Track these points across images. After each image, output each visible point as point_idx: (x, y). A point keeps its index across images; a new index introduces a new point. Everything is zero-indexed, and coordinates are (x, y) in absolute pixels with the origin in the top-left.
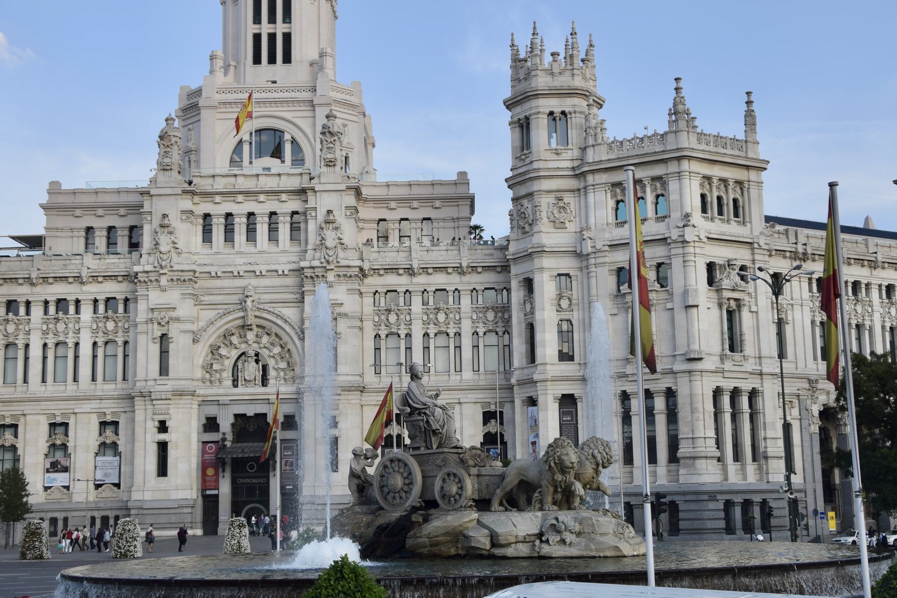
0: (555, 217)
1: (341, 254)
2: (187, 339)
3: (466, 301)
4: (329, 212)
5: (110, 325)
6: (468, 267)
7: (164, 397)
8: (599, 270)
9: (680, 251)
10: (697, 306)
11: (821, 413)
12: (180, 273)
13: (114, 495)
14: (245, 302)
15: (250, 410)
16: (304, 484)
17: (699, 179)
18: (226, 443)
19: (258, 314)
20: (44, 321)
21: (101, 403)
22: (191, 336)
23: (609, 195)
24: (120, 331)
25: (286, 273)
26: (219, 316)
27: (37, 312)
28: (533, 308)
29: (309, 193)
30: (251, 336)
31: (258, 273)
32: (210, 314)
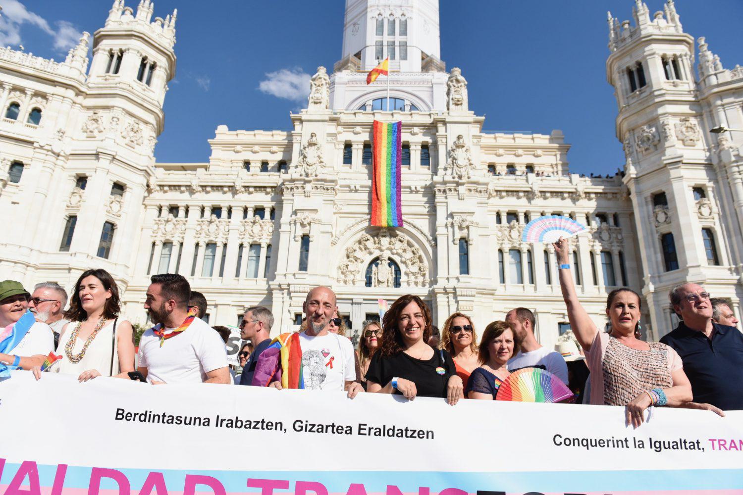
1: (471, 173)
2: (328, 239)
4: (459, 137)
5: (256, 228)
12: (323, 183)
20: (199, 223)
21: (241, 297)
26: (357, 221)
29: (440, 125)
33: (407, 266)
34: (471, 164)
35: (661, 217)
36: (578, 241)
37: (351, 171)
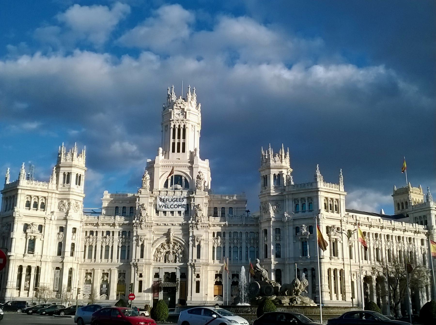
1: (202, 219)
3: (244, 236)
4: (199, 205)
6: (245, 225)
7: (142, 265)
8: (290, 227)
11: (364, 278)
13: (123, 298)
14: (170, 234)
15: (170, 271)
16: (188, 297)
18: (162, 282)
19: (174, 238)
23: (293, 202)
24: (127, 243)
25: (184, 224)
27: (100, 235)
28: (267, 239)
30: (171, 246)
33: (179, 255)
34: (203, 216)
35: (265, 238)
36: (242, 243)
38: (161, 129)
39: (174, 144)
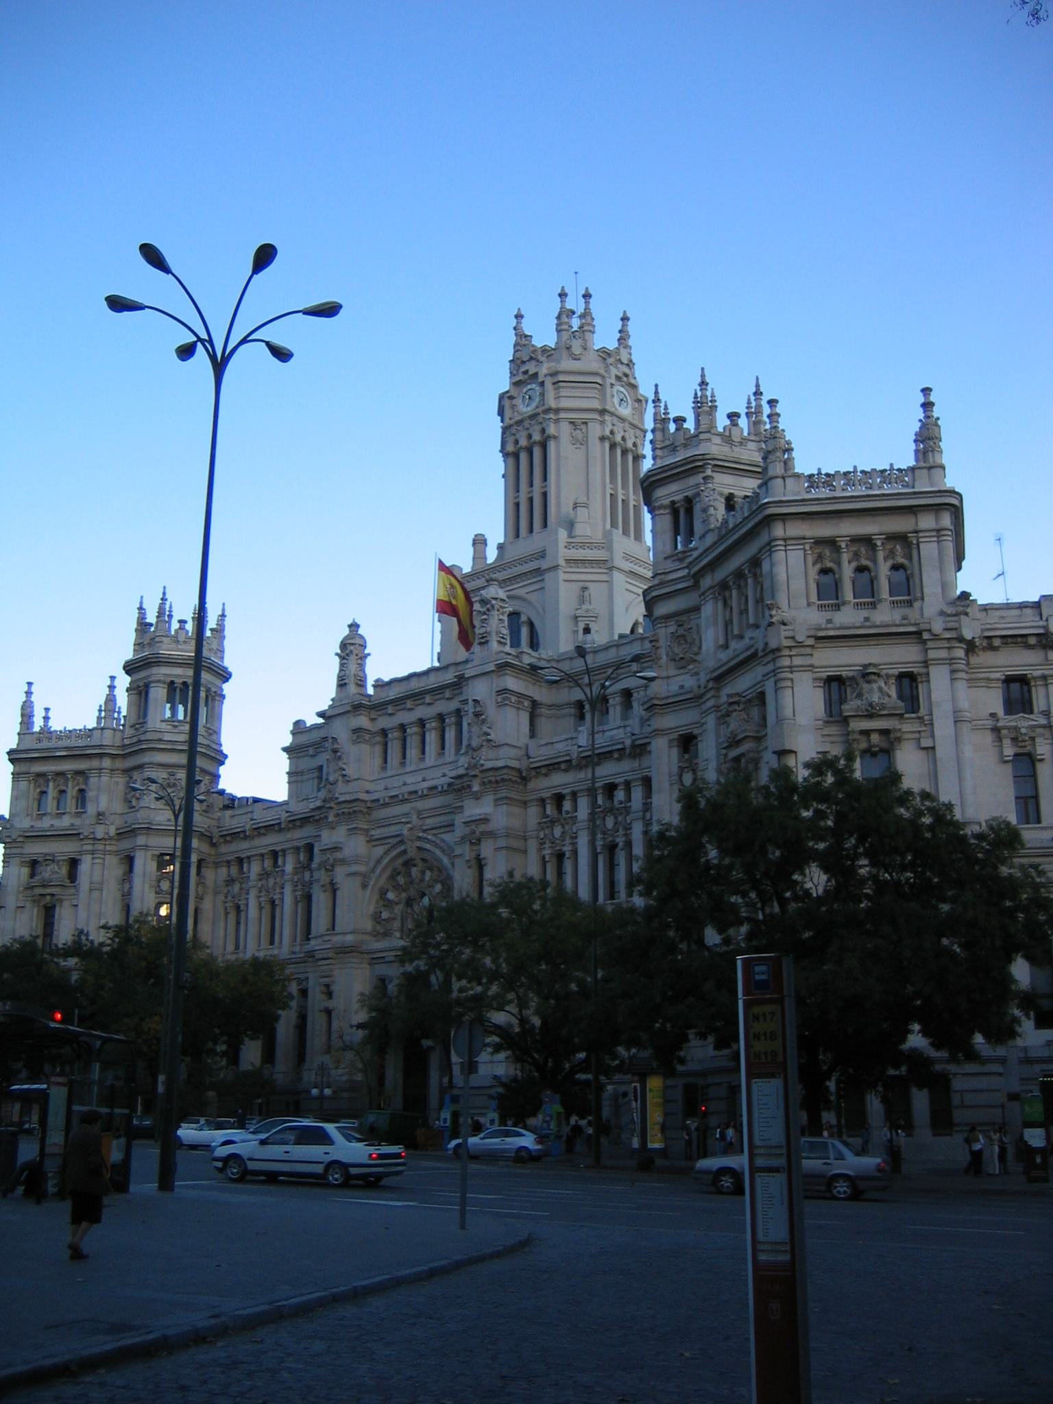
0: (673, 652)
6: (633, 746)
7: (325, 956)
9: (770, 667)
10: (795, 752)
17: (807, 547)
19: (418, 844)
22: (358, 881)
23: (720, 605)
27: (255, 868)
30: (414, 871)
31: (420, 793)
32: (379, 851)
36: (630, 829)
37: (384, 775)
38: (503, 472)
39: (517, 505)
